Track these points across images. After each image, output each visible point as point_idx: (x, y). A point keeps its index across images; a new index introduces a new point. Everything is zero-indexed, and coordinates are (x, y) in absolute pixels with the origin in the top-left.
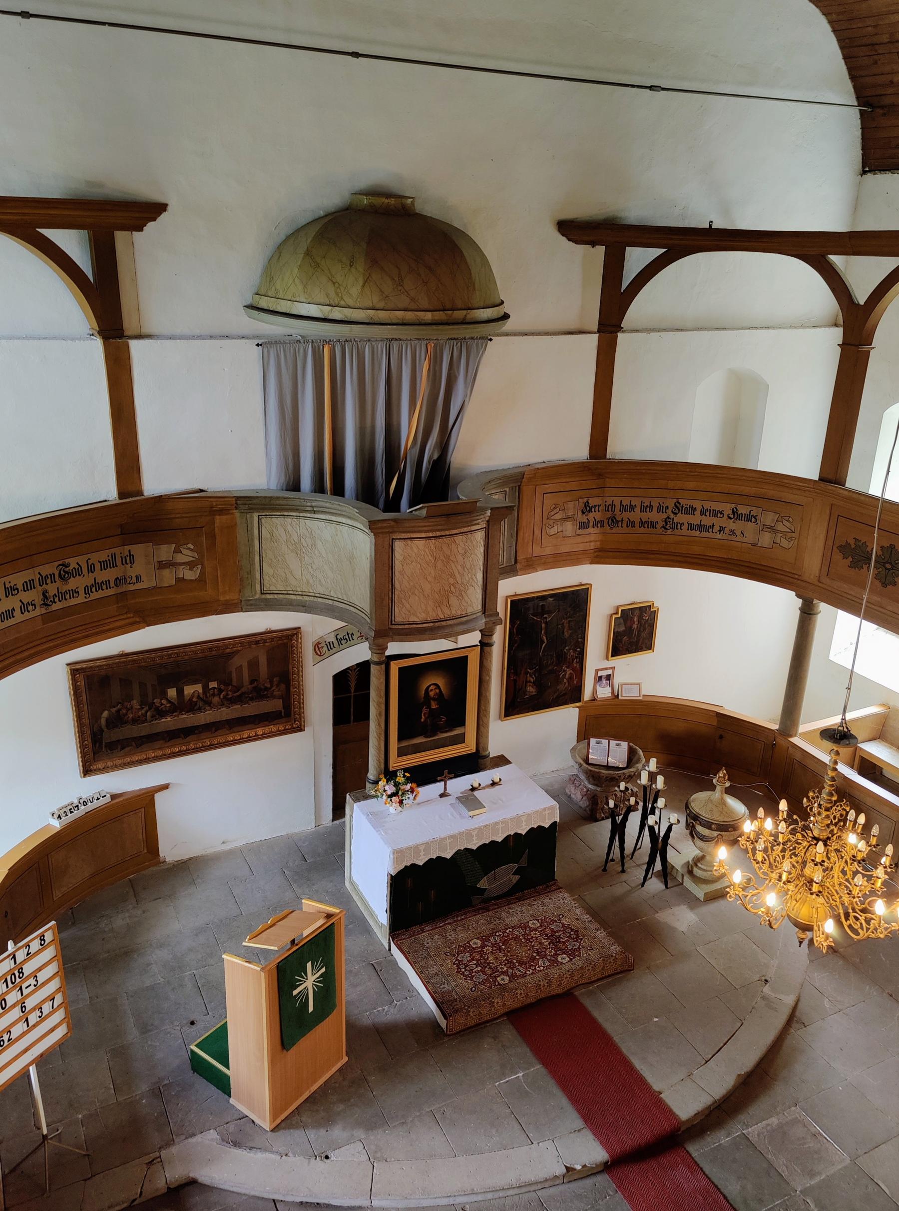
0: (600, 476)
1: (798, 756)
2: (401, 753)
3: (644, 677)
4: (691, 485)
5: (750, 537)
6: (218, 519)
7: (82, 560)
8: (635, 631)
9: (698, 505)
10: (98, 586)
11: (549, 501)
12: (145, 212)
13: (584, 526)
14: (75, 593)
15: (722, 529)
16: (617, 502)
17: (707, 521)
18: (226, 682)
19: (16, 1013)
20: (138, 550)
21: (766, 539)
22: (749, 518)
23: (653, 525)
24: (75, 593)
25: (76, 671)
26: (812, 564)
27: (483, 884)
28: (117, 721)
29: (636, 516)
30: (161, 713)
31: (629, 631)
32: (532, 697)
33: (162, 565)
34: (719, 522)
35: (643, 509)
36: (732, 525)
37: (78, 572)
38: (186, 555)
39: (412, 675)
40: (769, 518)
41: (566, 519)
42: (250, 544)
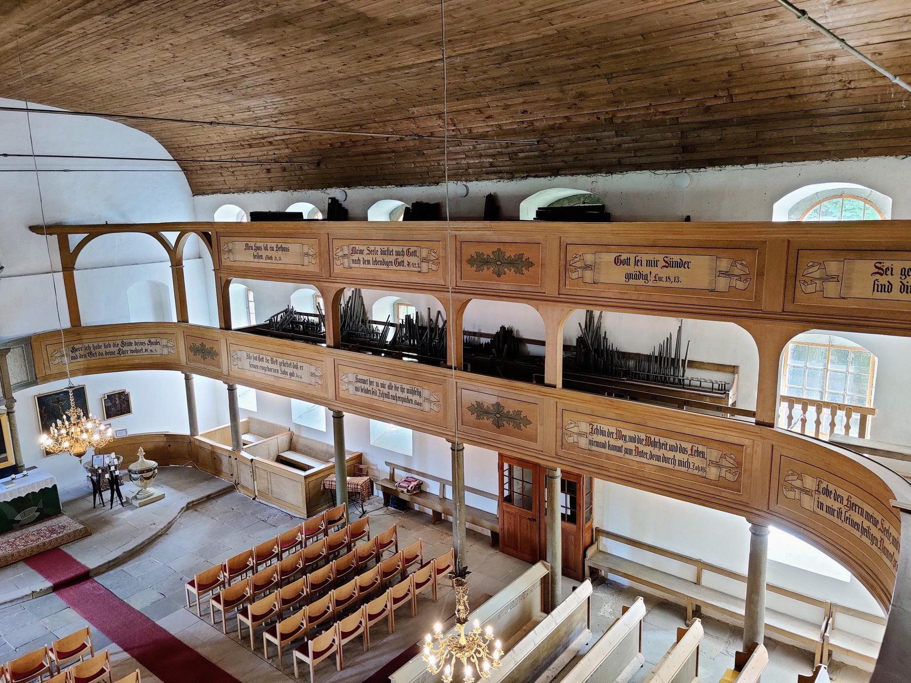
0: (78, 334)
1: (198, 444)
4: (127, 333)
5: (159, 352)
8: (118, 405)
9: (132, 341)
13: (73, 358)
15: (146, 350)
16: (91, 345)
17: (139, 348)
21: (165, 351)
22: (157, 343)
23: (113, 353)
26: (183, 359)
27: (18, 517)
29: (103, 350)
34: (144, 347)
35: (106, 347)
36: (150, 348)
40: (164, 342)
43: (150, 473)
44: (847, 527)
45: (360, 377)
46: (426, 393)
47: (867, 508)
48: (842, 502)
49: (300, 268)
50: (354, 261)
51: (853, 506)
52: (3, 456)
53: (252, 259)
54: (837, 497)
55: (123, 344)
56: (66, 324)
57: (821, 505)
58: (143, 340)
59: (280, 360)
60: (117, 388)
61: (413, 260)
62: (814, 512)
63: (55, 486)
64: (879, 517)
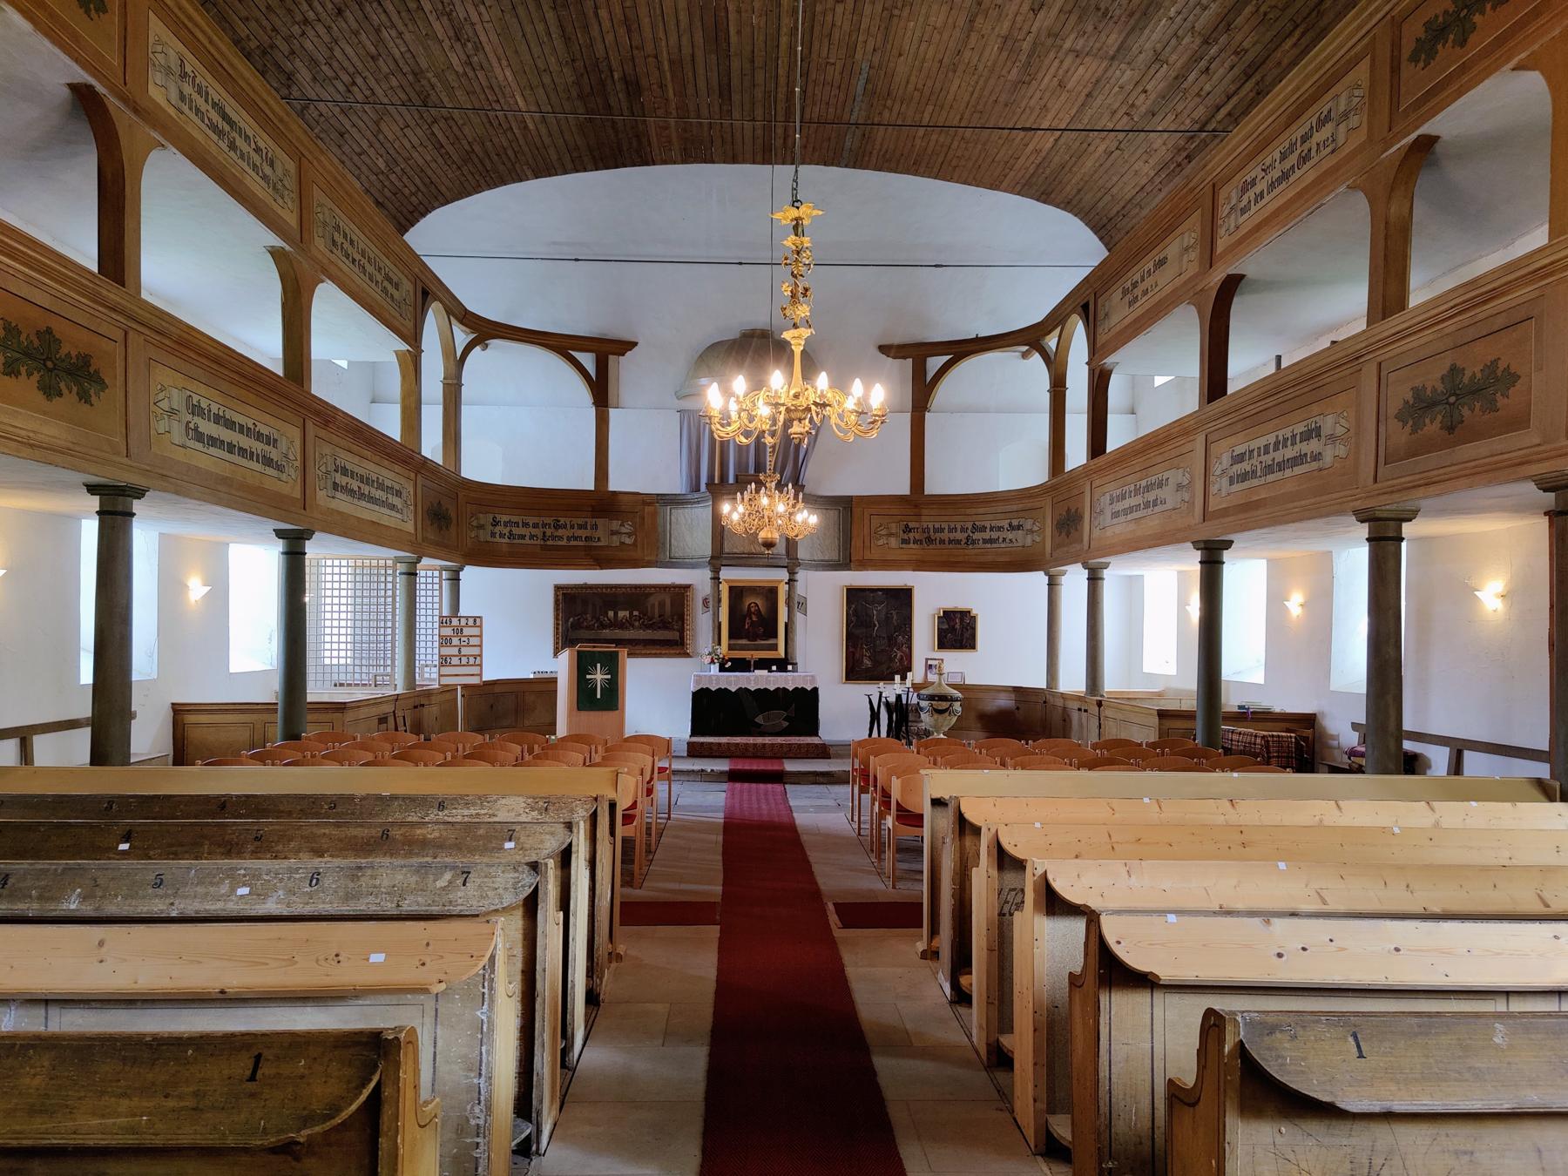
2: (731, 648)
3: (962, 667)
4: (981, 511)
6: (647, 509)
7: (568, 521)
8: (958, 630)
10: (576, 538)
11: (876, 521)
12: (624, 346)
13: (905, 541)
14: (561, 538)
17: (994, 535)
18: (644, 613)
19: (455, 651)
20: (600, 522)
22: (1019, 527)
23: (959, 542)
24: (561, 538)
25: (558, 588)
27: (759, 720)
28: (577, 626)
29: (945, 535)
30: (603, 626)
31: (953, 629)
32: (868, 670)
33: (613, 533)
34: (1002, 535)
35: (950, 530)
36: (1010, 535)
37: (565, 527)
38: (627, 528)
39: (737, 593)
41: (890, 535)
42: (664, 526)
43: (944, 705)
45: (1239, 450)
46: (1328, 424)
49: (1178, 282)
50: (1243, 211)
52: (771, 641)
53: (1127, 311)
55: (975, 529)
56: (904, 488)
58: (1000, 524)
59: (1144, 483)
60: (961, 605)
61: (1327, 131)
63: (815, 690)
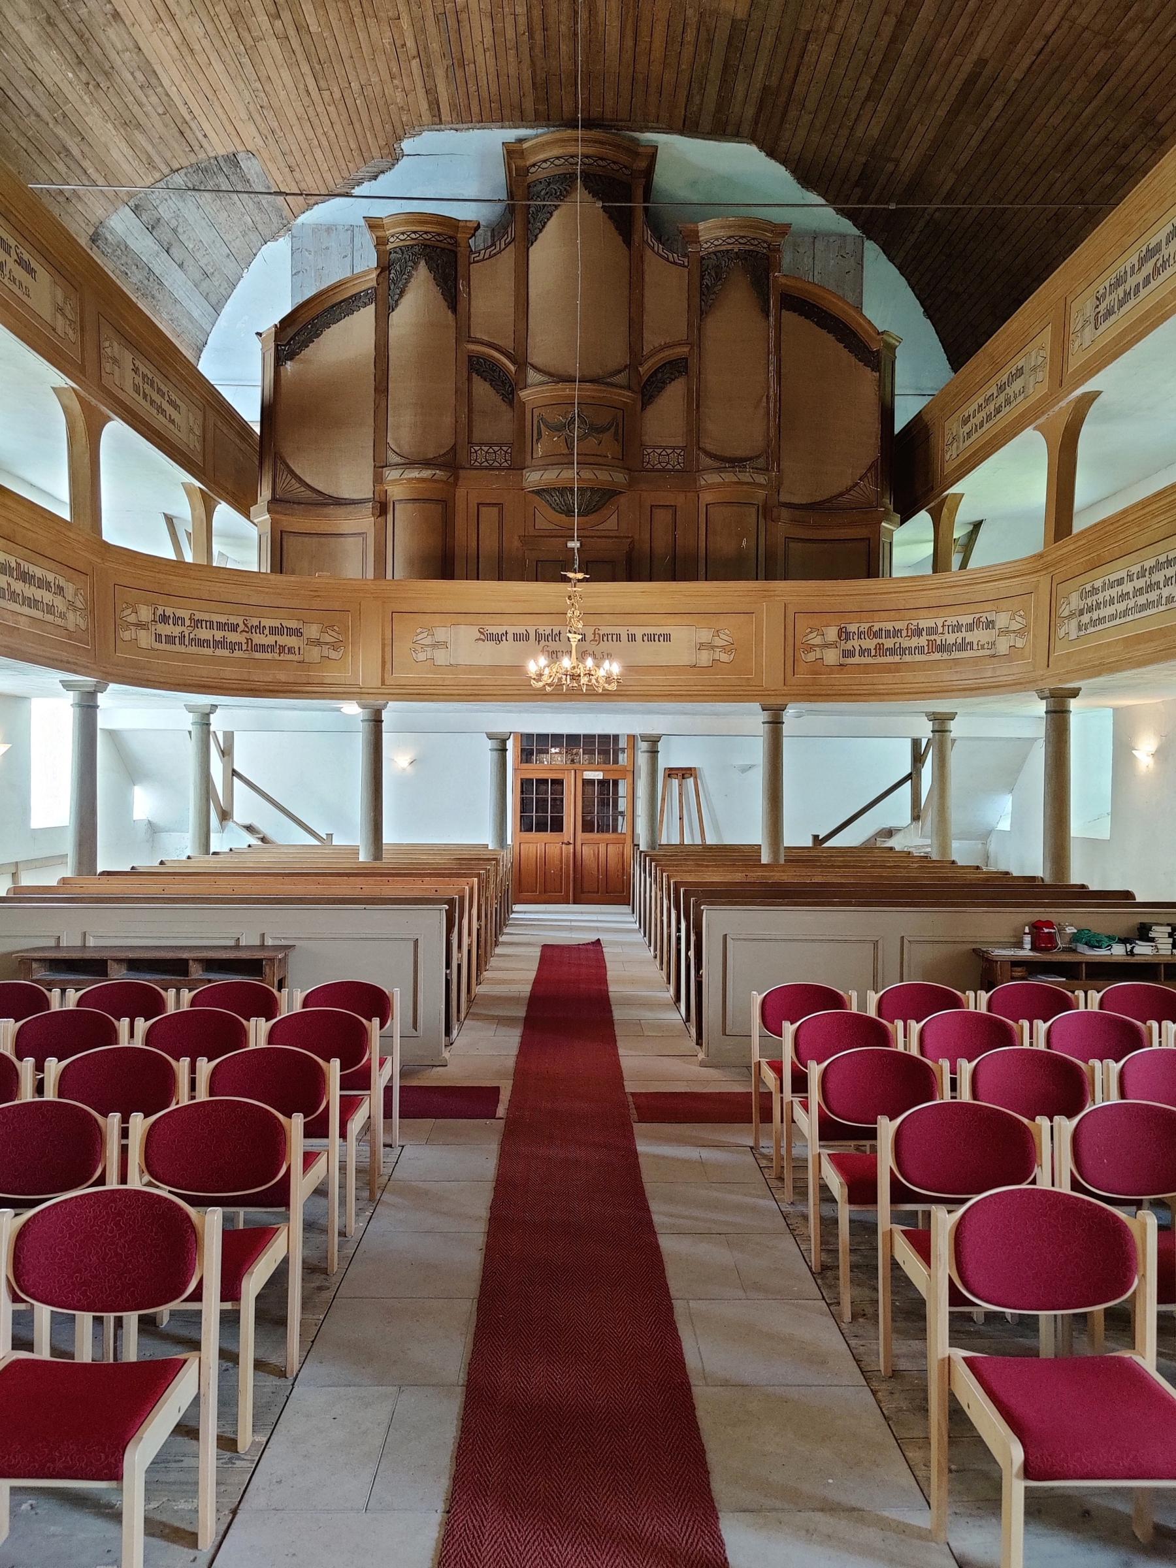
44: (194, 649)
47: (216, 618)
48: (183, 624)
51: (197, 623)
54: (177, 620)
57: (158, 637)
62: (153, 649)
64: (233, 620)
